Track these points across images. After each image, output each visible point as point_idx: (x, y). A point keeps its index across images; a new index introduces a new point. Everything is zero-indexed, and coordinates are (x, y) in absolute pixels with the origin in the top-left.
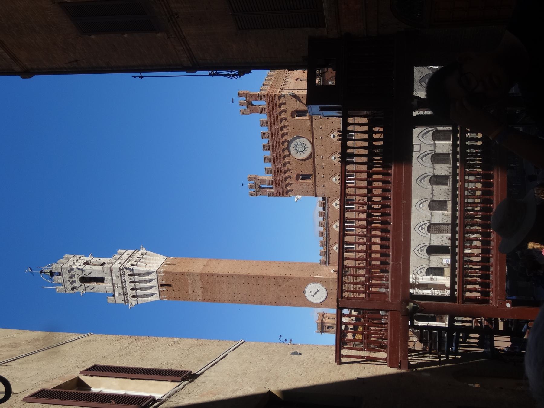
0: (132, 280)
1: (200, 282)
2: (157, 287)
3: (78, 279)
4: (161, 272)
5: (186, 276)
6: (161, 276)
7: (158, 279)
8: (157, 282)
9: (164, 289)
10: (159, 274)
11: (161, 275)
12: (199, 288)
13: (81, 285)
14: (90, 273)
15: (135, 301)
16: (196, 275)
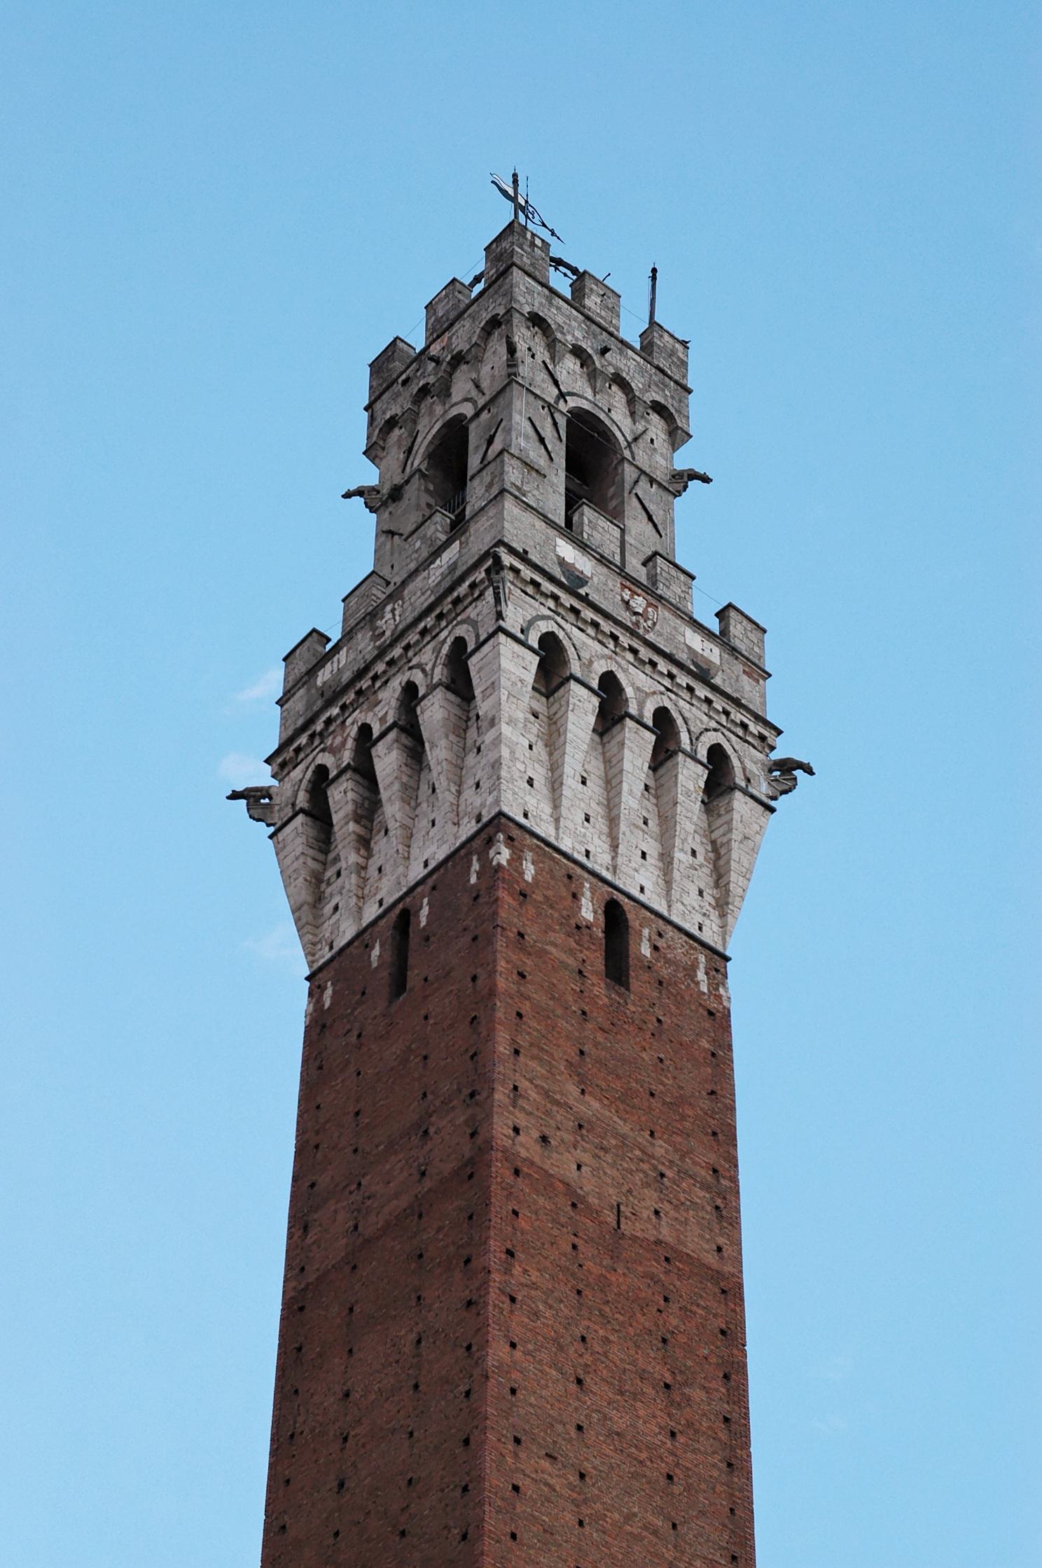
0: (684, 737)
1: (666, 1233)
2: (608, 875)
3: (602, 416)
4: (721, 991)
5: (712, 1158)
6: (694, 967)
7: (670, 932)
8: (642, 898)
9: (588, 911)
10: (702, 959)
11: (701, 975)
12: (613, 1195)
13: (562, 395)
14: (650, 518)
15: (522, 631)
16: (721, 1241)
